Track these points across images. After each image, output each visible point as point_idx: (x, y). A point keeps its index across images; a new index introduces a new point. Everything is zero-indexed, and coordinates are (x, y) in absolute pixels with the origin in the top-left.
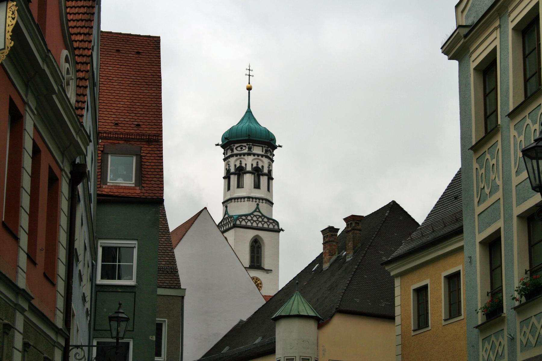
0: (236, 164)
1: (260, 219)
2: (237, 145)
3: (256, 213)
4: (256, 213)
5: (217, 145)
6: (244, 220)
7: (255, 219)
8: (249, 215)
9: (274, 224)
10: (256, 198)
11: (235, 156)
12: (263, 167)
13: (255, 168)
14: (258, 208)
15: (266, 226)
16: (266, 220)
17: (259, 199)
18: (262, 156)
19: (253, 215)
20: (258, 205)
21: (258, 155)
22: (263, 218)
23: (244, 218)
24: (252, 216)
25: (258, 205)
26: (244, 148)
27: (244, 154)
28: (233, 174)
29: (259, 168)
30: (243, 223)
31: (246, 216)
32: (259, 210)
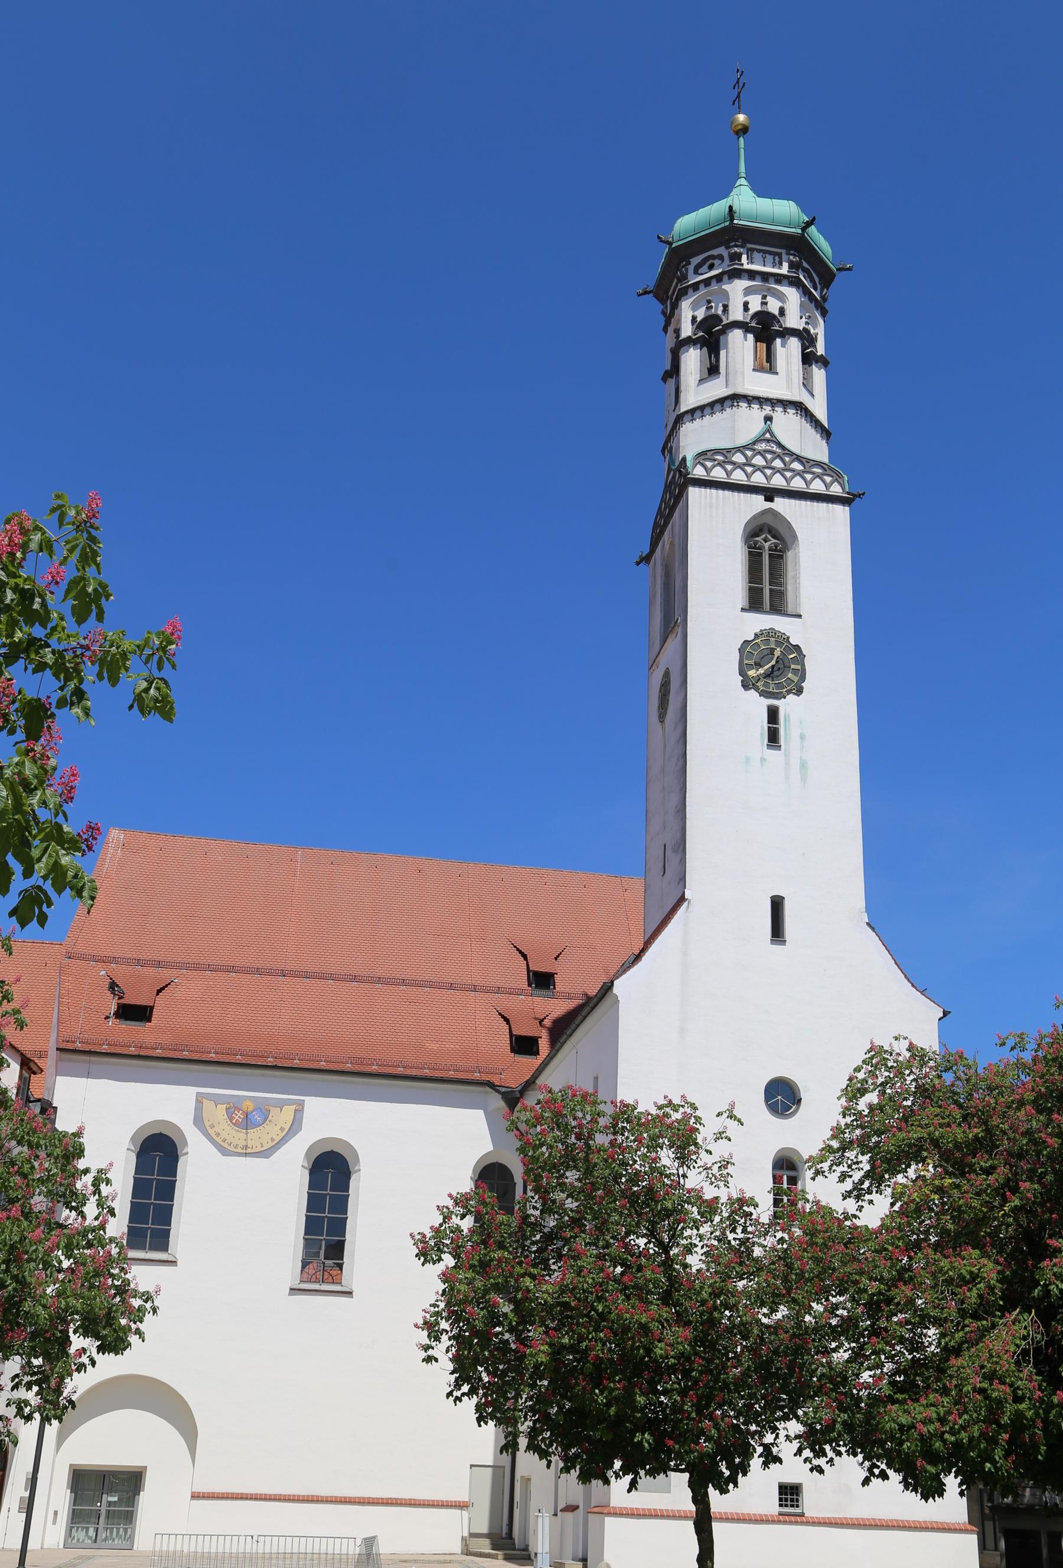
0: (696, 313)
1: (778, 464)
2: (696, 260)
3: (762, 446)
4: (762, 446)
5: (646, 293)
6: (721, 464)
7: (758, 461)
8: (740, 449)
9: (828, 479)
10: (761, 401)
11: (690, 291)
12: (782, 311)
13: (757, 315)
14: (769, 430)
15: (798, 484)
16: (797, 466)
17: (773, 402)
18: (779, 279)
19: (754, 450)
20: (768, 419)
21: (765, 277)
22: (787, 459)
23: (720, 458)
24: (749, 453)
25: (768, 419)
26: (717, 262)
27: (719, 278)
28: (689, 341)
29: (774, 316)
30: (718, 474)
31: (727, 452)
32: (772, 434)
